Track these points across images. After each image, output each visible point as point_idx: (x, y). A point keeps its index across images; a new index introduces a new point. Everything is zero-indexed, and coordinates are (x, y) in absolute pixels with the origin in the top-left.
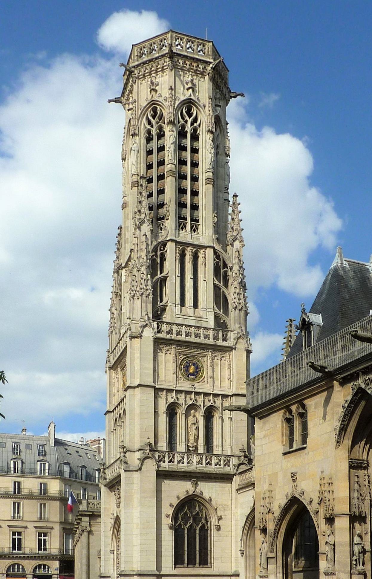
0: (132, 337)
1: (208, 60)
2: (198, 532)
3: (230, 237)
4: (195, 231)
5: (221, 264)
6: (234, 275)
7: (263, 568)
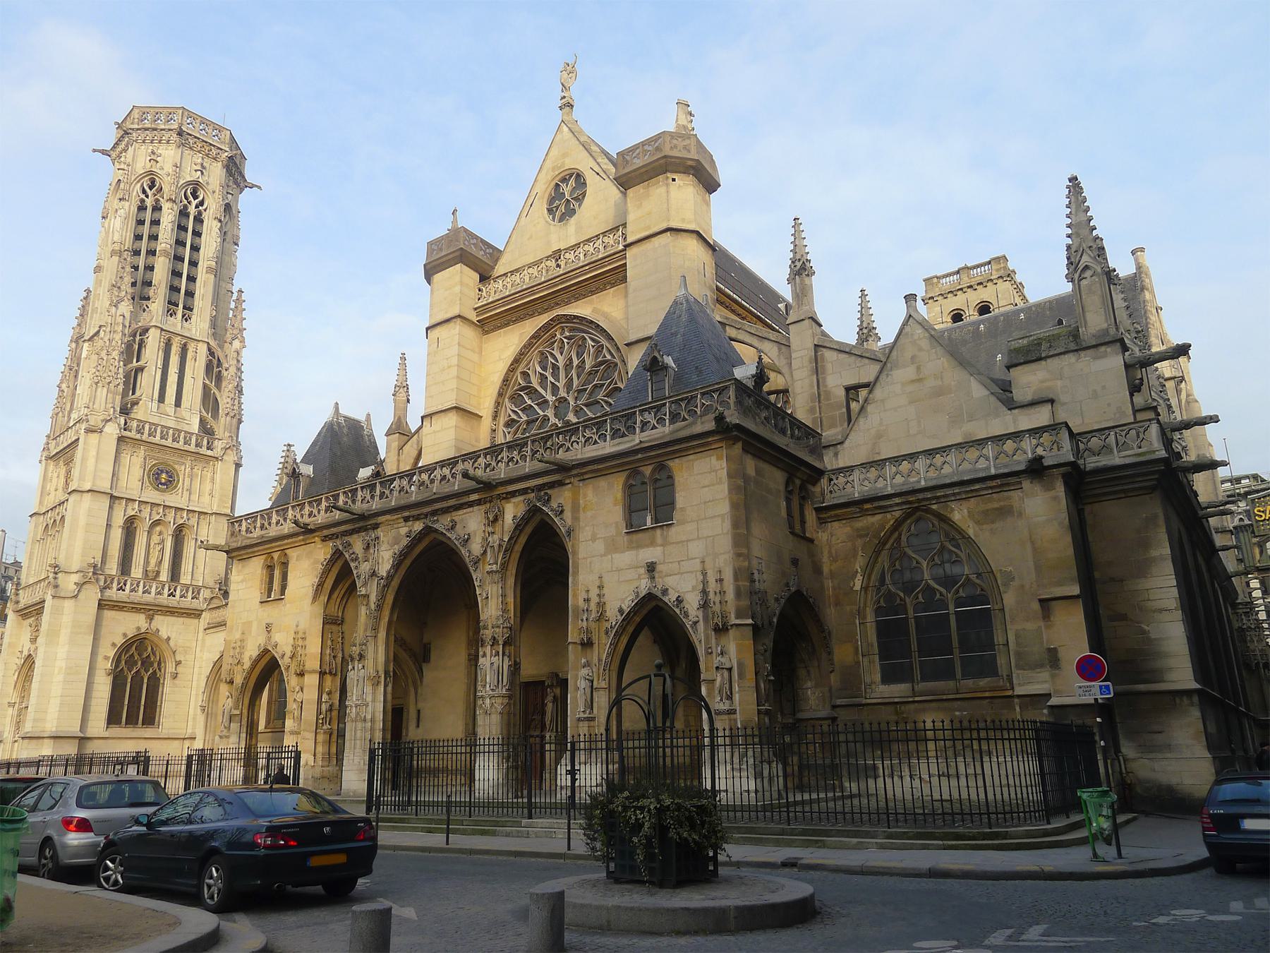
0: (88, 431)
1: (223, 148)
2: (146, 681)
3: (229, 337)
4: (186, 320)
5: (215, 362)
7: (225, 728)
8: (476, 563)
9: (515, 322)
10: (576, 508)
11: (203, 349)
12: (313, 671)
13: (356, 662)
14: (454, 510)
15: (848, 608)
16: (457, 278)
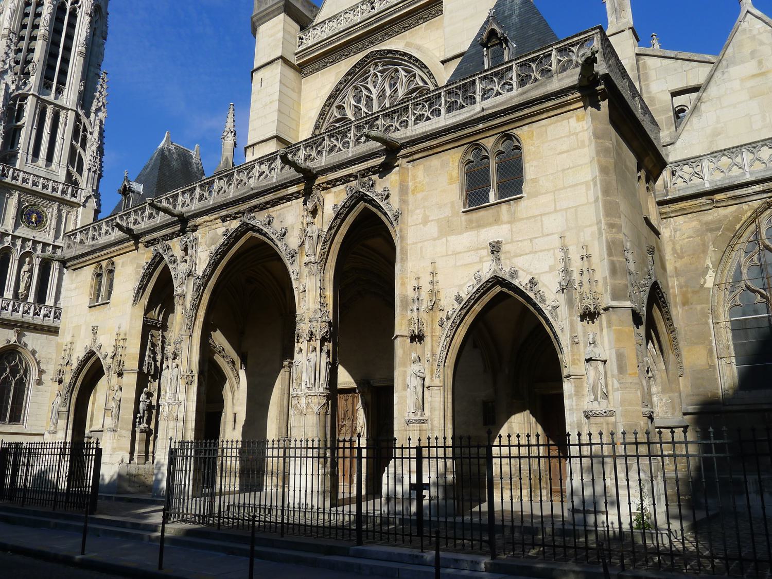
5: (81, 127)
6: (93, 140)
8: (293, 256)
9: (331, 63)
10: (404, 190)
11: (71, 116)
12: (132, 371)
13: (170, 361)
14: (273, 206)
15: (699, 307)
16: (281, 26)
